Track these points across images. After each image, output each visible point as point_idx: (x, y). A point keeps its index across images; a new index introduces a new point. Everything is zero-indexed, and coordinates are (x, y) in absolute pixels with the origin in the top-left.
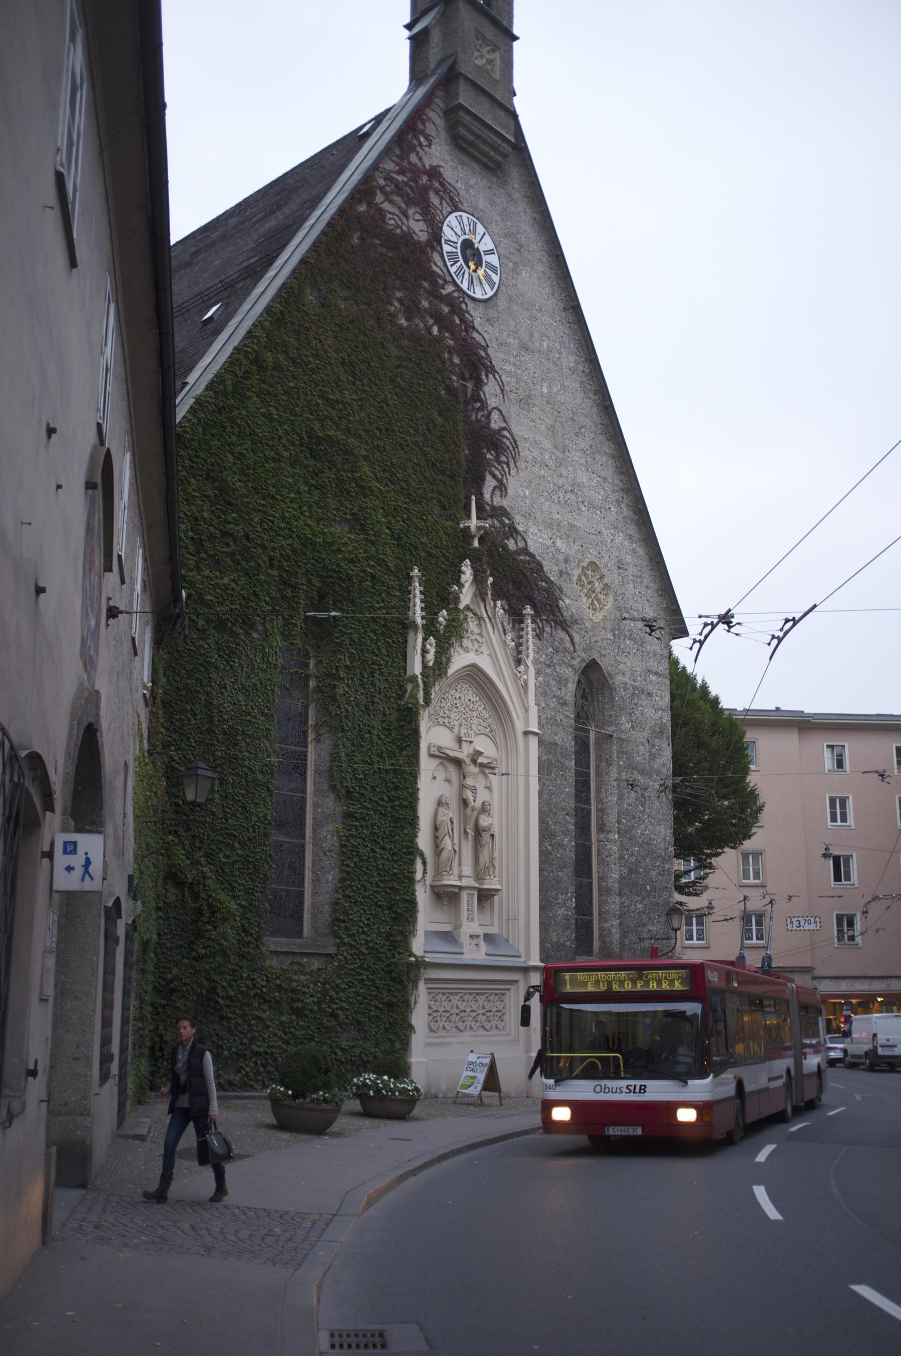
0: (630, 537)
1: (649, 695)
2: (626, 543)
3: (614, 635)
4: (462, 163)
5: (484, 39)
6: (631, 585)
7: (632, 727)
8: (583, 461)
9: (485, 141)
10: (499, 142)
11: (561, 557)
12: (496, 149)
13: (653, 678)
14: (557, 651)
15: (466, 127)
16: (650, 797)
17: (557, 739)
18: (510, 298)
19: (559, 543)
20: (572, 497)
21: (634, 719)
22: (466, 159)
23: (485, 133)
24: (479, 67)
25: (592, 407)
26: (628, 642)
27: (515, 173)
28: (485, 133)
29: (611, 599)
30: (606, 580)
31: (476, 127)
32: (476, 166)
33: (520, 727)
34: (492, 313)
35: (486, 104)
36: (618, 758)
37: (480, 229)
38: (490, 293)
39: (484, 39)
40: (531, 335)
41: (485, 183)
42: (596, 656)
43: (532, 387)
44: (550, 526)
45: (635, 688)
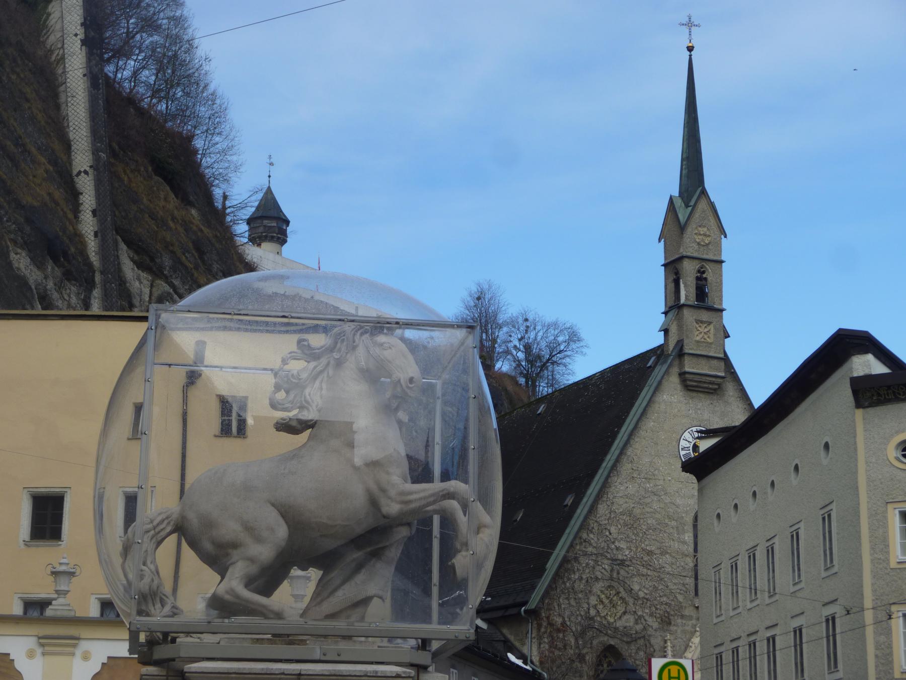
4: (692, 398)
5: (702, 322)
9: (705, 382)
15: (691, 381)
22: (694, 394)
23: (704, 379)
24: (698, 342)
27: (730, 389)
28: (704, 379)
31: (697, 378)
32: (701, 395)
35: (703, 361)
39: (702, 322)
41: (709, 402)
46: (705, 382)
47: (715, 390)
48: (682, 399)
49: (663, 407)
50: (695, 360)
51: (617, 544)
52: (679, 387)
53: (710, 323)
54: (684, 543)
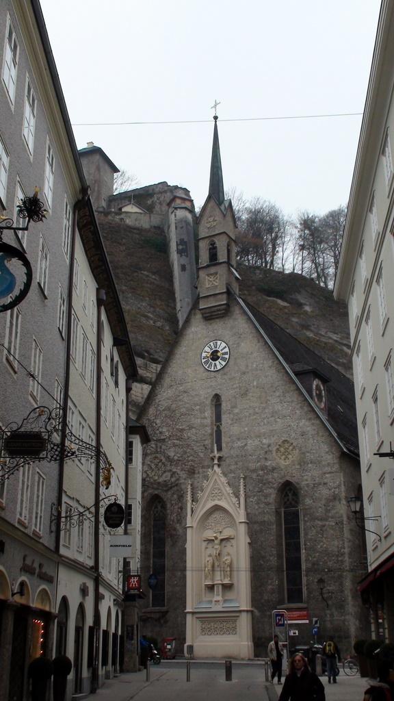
0: (310, 419)
1: (325, 484)
2: (307, 423)
3: (301, 466)
4: (211, 324)
5: (211, 274)
6: (311, 440)
7: (314, 502)
8: (279, 400)
9: (215, 311)
10: (219, 308)
11: (265, 446)
12: (220, 310)
13: (327, 475)
14: (265, 484)
16: (326, 530)
17: (266, 519)
18: (236, 359)
19: (264, 441)
20: (273, 419)
21: (314, 497)
22: (212, 321)
25: (283, 375)
26: (310, 465)
29: (298, 451)
30: (294, 444)
31: (207, 311)
32: (217, 320)
33: (237, 522)
34: (226, 370)
35: (211, 299)
36: (304, 516)
37: (219, 342)
38: (224, 363)
39: (211, 274)
40: (247, 366)
42: (288, 478)
43: (247, 386)
44: (259, 436)
45: (314, 484)
46: (215, 311)
47: (223, 313)
48: (204, 327)
49: (191, 336)
50: (205, 300)
51: (160, 430)
52: (202, 320)
53: (216, 273)
54: (205, 418)
